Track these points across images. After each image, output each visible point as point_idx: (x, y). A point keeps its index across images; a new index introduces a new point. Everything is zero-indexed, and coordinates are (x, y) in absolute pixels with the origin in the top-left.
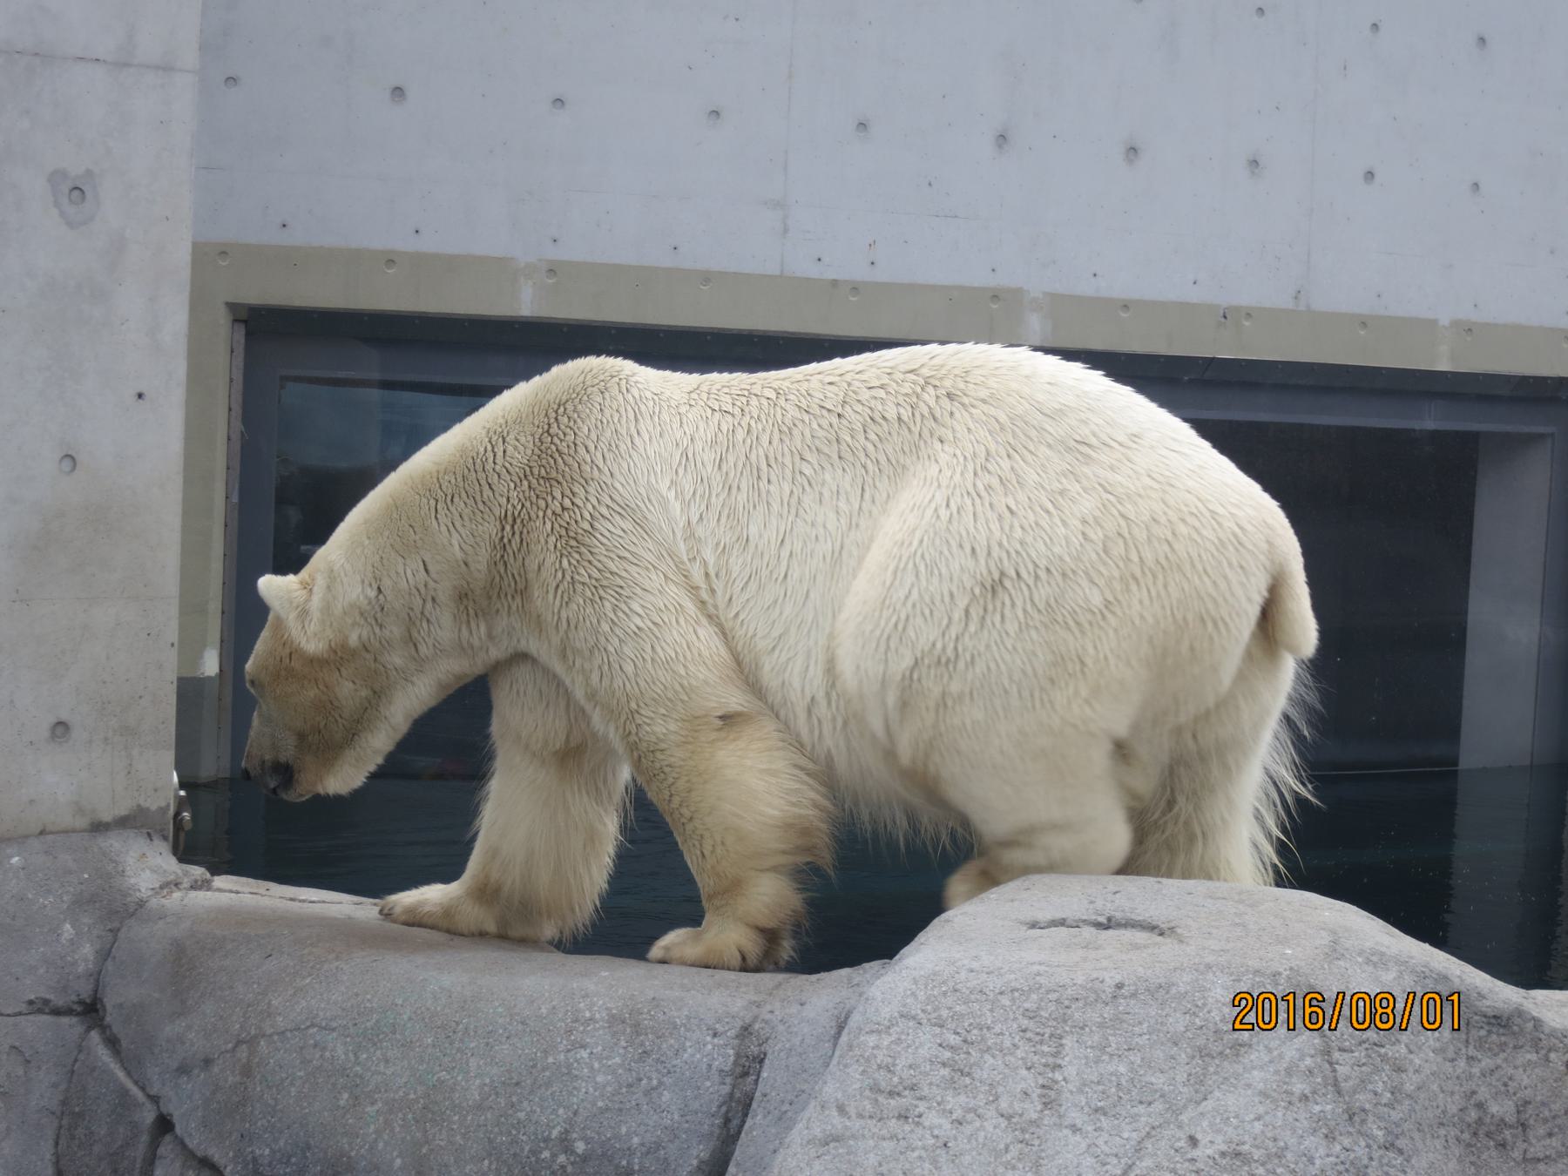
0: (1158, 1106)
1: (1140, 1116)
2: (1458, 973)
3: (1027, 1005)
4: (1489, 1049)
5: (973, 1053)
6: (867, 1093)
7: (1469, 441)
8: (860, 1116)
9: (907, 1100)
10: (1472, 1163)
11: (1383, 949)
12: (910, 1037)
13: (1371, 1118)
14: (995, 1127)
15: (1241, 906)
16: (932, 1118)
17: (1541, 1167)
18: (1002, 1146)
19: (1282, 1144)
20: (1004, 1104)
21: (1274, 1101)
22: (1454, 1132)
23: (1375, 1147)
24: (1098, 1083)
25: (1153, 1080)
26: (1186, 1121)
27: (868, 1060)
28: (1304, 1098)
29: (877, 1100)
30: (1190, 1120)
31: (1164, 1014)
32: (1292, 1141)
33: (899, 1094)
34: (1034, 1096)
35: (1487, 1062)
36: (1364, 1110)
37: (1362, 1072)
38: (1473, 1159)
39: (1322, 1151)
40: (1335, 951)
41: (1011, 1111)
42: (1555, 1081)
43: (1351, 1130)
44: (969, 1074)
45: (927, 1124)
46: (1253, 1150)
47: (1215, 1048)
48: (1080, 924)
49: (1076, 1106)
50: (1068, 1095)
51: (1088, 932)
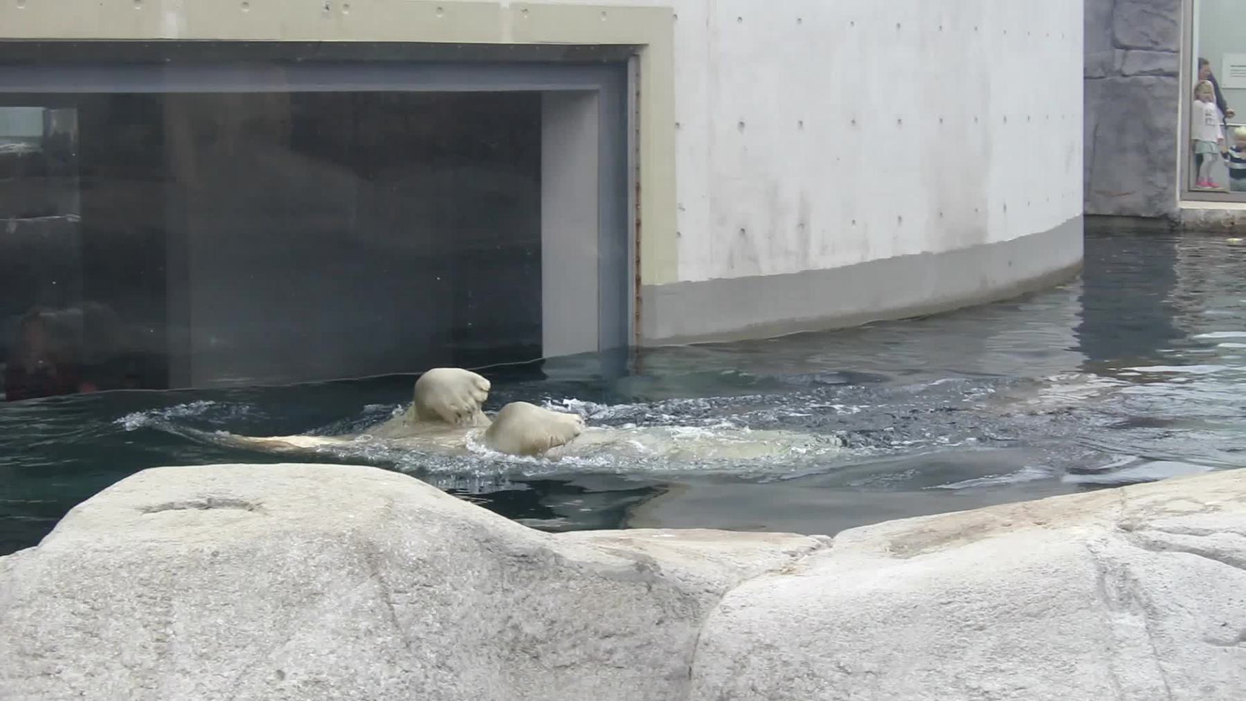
0: (251, 649)
1: (236, 658)
2: (492, 523)
3: (141, 575)
4: (520, 581)
5: (100, 618)
6: (16, 657)
7: (535, 98)
8: (12, 676)
9: (49, 660)
10: (512, 674)
11: (430, 509)
12: (48, 609)
13: (424, 645)
14: (121, 677)
15: (315, 483)
16: (69, 673)
17: (568, 671)
18: (127, 691)
19: (353, 671)
20: (127, 657)
21: (345, 637)
22: (495, 650)
23: (429, 667)
24: (202, 634)
25: (246, 628)
26: (274, 659)
27: (14, 630)
28: (369, 633)
29: (24, 663)
30: (277, 658)
31: (252, 574)
32: (361, 668)
33: (41, 656)
34: (151, 648)
35: (519, 593)
36: (418, 638)
37: (414, 609)
38: (512, 670)
39: (385, 674)
40: (390, 513)
41: (133, 663)
42: (576, 604)
43: (410, 655)
44: (97, 636)
45: (65, 678)
46: (330, 678)
47: (294, 598)
48: (186, 506)
49: (185, 654)
50: (178, 646)
51: (192, 512)
